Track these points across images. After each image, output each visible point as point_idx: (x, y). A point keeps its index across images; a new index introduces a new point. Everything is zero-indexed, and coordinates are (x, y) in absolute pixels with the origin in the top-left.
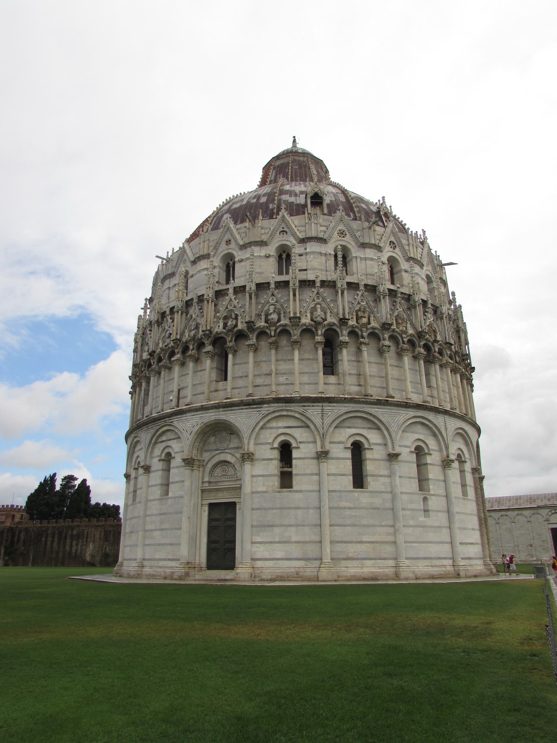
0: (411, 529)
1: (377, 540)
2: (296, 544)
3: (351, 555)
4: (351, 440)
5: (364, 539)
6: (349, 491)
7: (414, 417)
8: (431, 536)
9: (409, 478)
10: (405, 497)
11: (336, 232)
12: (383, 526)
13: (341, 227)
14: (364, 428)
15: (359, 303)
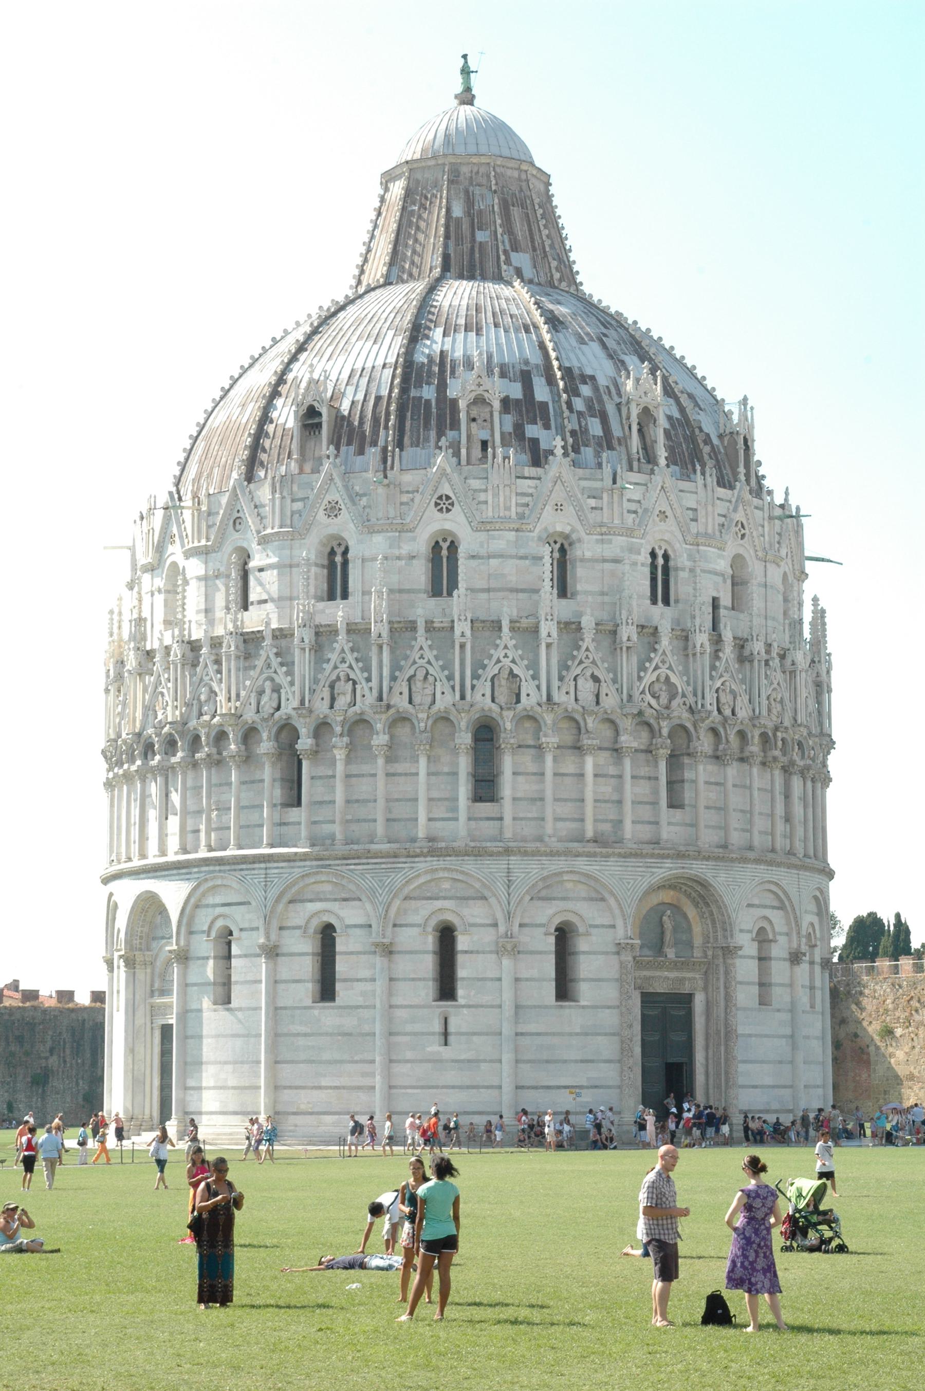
0: (409, 1065)
1: (344, 1084)
2: (232, 1091)
3: (303, 1107)
4: (315, 923)
5: (323, 1084)
6: (305, 1008)
7: (426, 872)
8: (451, 1076)
9: (413, 979)
10: (399, 1013)
11: (323, 507)
12: (356, 1062)
13: (334, 495)
14: (335, 900)
15: (336, 667)
